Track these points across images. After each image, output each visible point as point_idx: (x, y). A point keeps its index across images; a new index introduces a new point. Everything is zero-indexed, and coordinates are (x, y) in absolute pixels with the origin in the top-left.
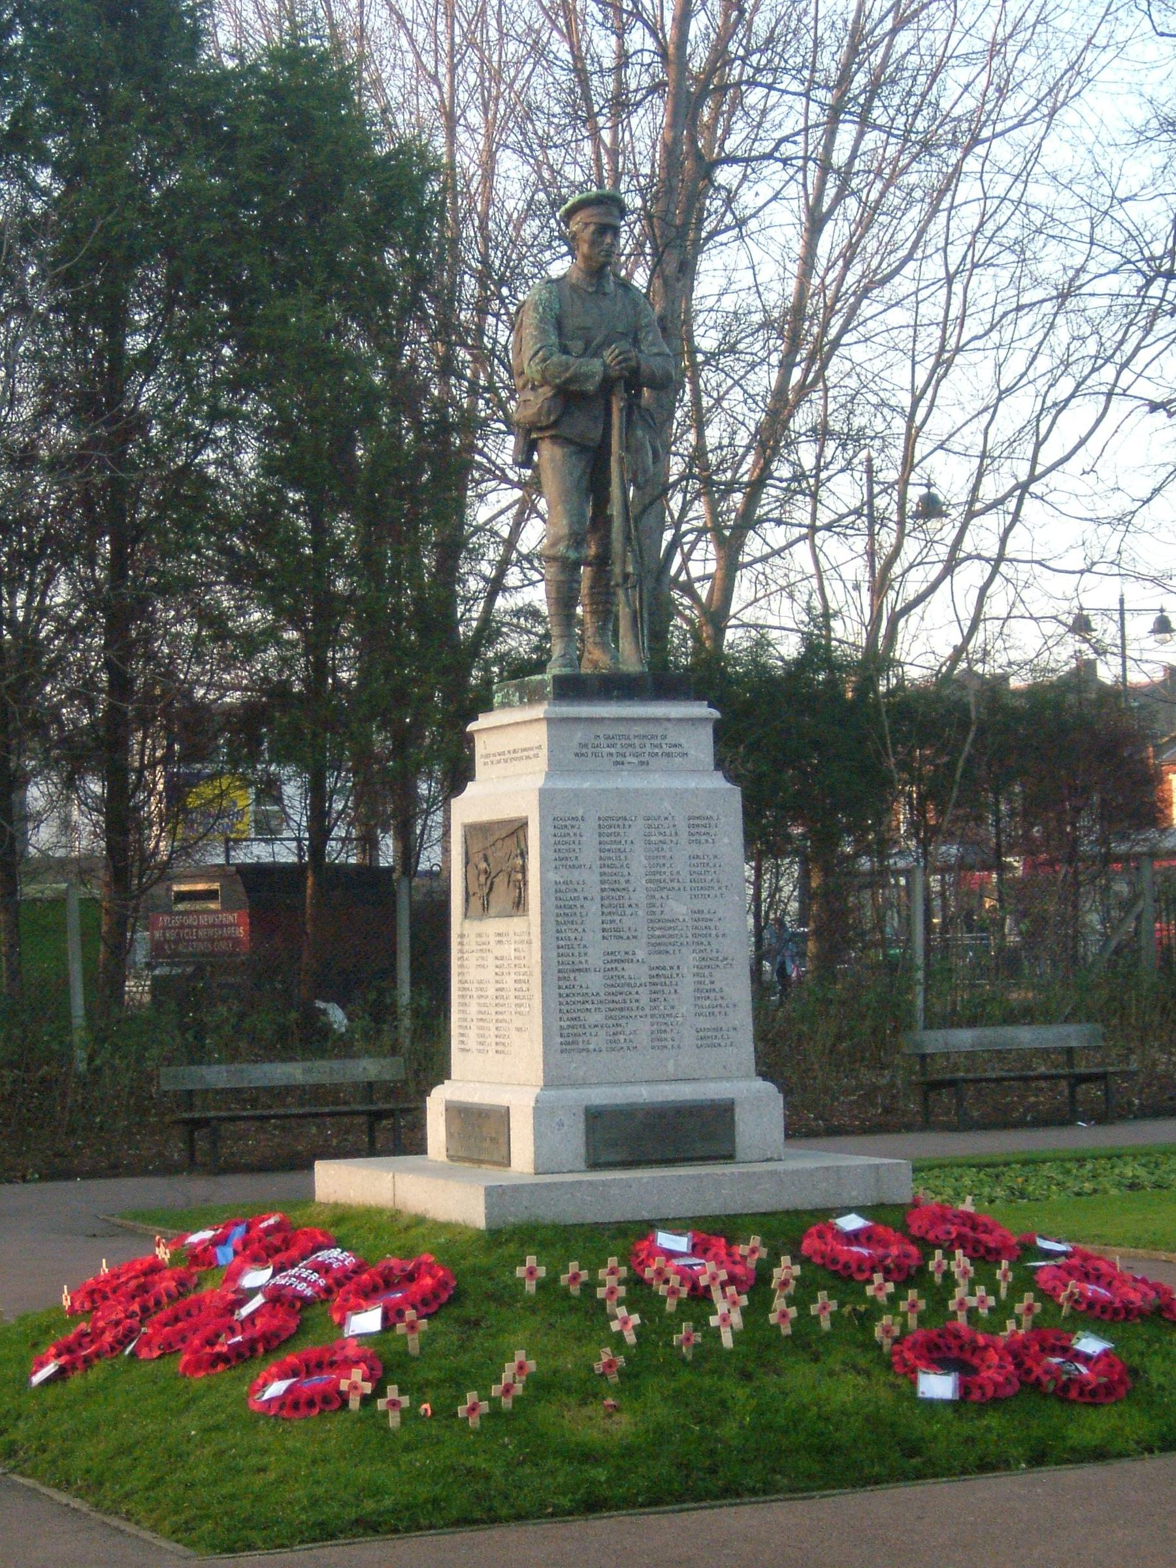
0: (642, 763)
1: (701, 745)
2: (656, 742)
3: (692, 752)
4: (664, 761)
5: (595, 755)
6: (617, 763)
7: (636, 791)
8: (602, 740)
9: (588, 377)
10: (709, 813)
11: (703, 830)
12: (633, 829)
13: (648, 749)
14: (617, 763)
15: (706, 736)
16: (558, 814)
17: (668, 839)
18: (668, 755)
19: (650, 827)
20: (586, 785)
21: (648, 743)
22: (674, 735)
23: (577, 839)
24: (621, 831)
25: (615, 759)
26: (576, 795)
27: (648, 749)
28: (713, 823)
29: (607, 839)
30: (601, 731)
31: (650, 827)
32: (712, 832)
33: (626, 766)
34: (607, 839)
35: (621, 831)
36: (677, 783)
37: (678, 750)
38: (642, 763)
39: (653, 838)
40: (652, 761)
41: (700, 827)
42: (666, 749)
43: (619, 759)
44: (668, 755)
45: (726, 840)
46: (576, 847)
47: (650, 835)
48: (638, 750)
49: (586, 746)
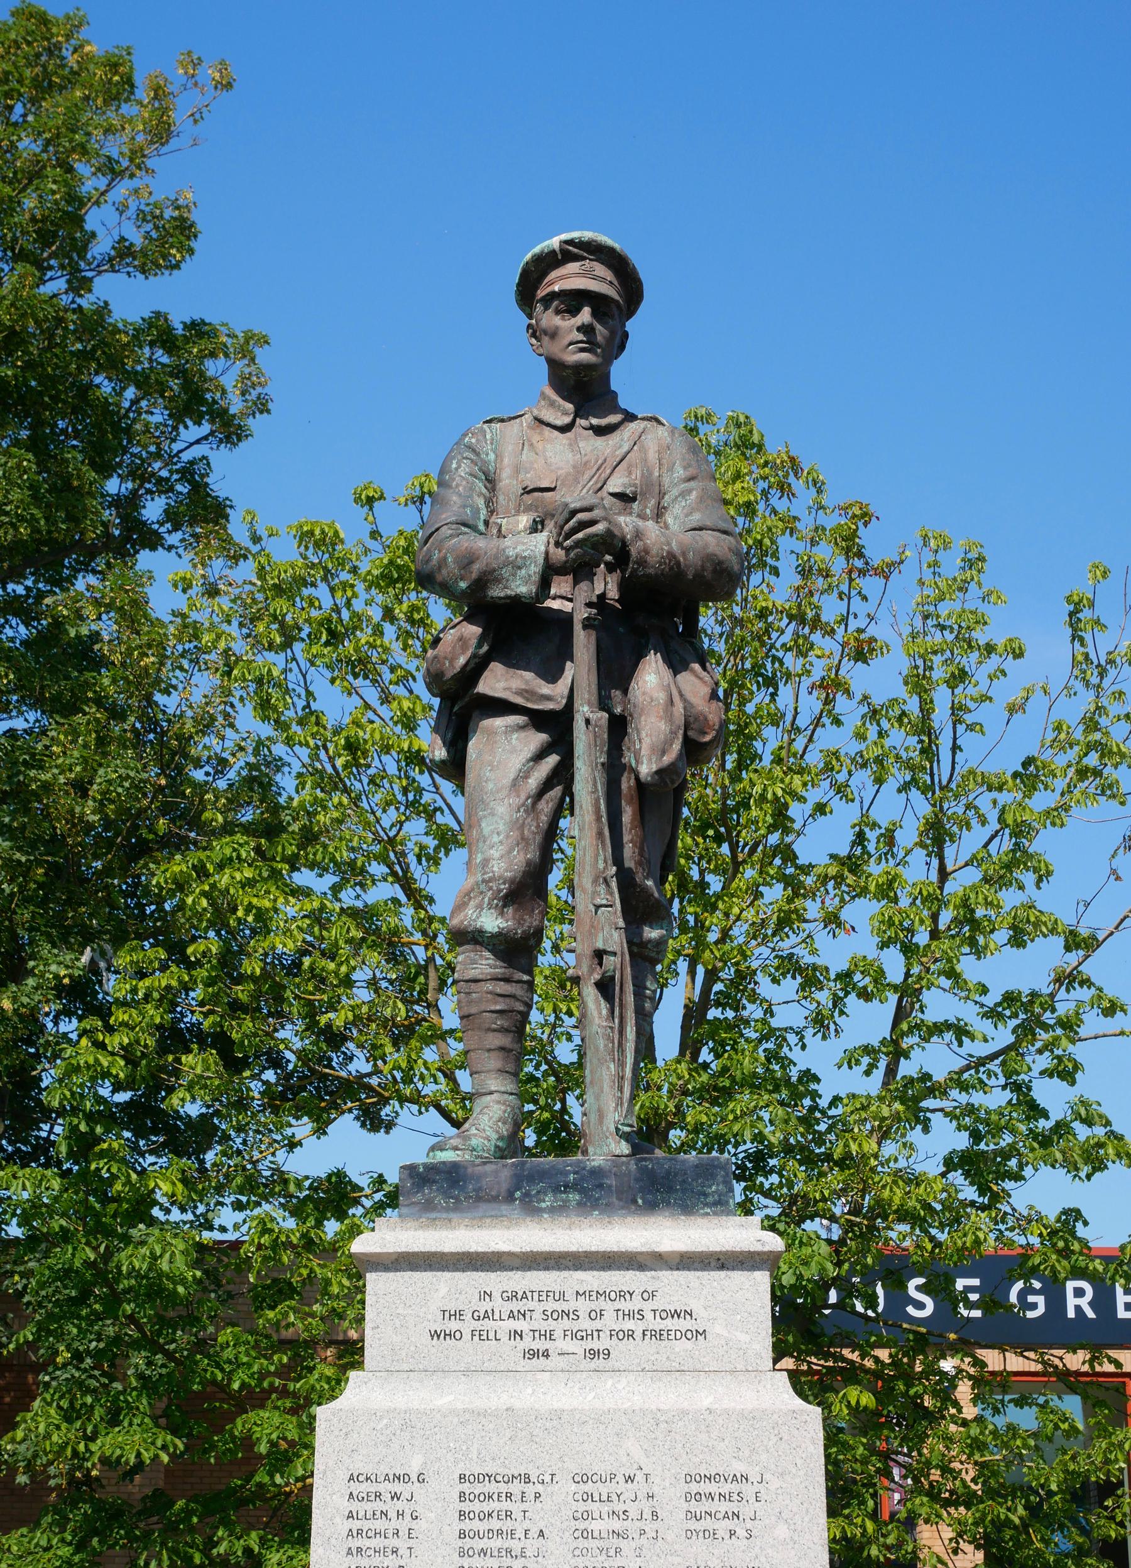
0: (594, 1354)
1: (743, 1309)
2: (625, 1305)
3: (717, 1329)
4: (651, 1345)
5: (480, 1335)
6: (534, 1354)
7: (557, 1414)
8: (498, 1304)
9: (516, 564)
10: (739, 1468)
11: (724, 1507)
12: (547, 1502)
13: (610, 1321)
14: (534, 1354)
15: (753, 1293)
16: (361, 1466)
17: (633, 1527)
18: (658, 1335)
19: (589, 1497)
20: (443, 1401)
21: (609, 1307)
22: (673, 1287)
23: (404, 1525)
24: (516, 1508)
25: (528, 1343)
26: (404, 1426)
27: (610, 1321)
28: (748, 1490)
29: (476, 1525)
30: (497, 1281)
31: (589, 1497)
32: (746, 1511)
33: (555, 1361)
34: (476, 1525)
35: (516, 1508)
36: (668, 1396)
37: (684, 1324)
38: (594, 1354)
39: (595, 1526)
40: (619, 1348)
41: (717, 1499)
42: (653, 1323)
43: (540, 1345)
44: (658, 1335)
45: (782, 1531)
46: (402, 1544)
47: (588, 1516)
48: (585, 1324)
49: (458, 1315)
